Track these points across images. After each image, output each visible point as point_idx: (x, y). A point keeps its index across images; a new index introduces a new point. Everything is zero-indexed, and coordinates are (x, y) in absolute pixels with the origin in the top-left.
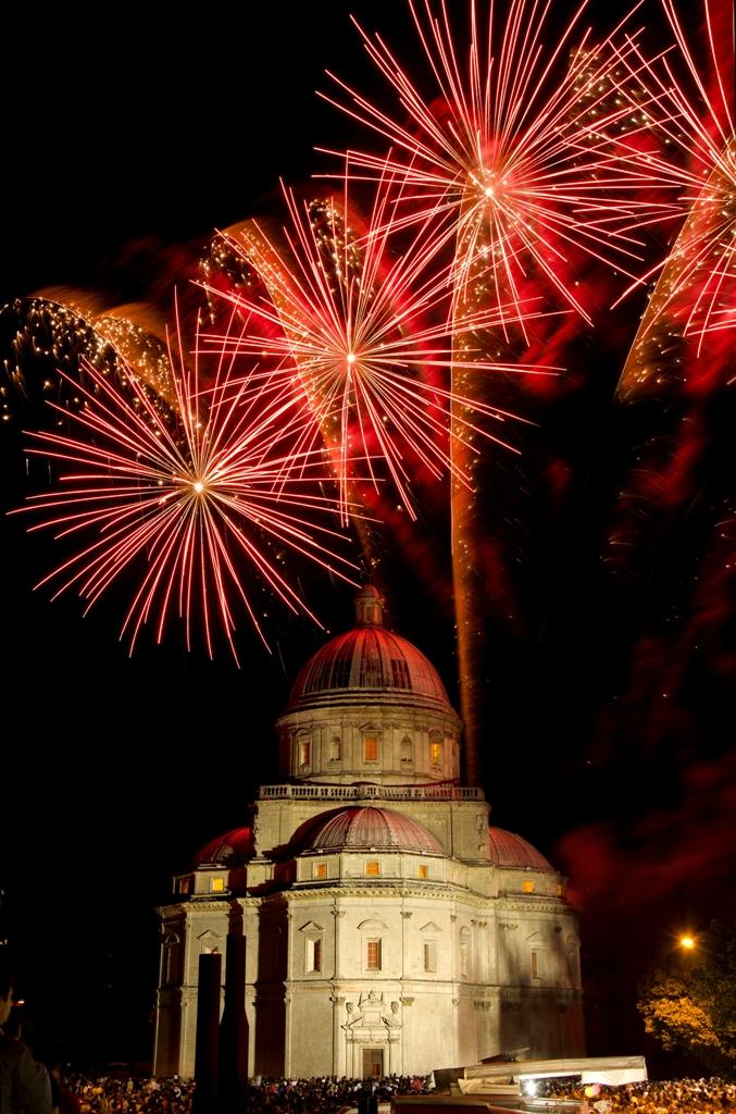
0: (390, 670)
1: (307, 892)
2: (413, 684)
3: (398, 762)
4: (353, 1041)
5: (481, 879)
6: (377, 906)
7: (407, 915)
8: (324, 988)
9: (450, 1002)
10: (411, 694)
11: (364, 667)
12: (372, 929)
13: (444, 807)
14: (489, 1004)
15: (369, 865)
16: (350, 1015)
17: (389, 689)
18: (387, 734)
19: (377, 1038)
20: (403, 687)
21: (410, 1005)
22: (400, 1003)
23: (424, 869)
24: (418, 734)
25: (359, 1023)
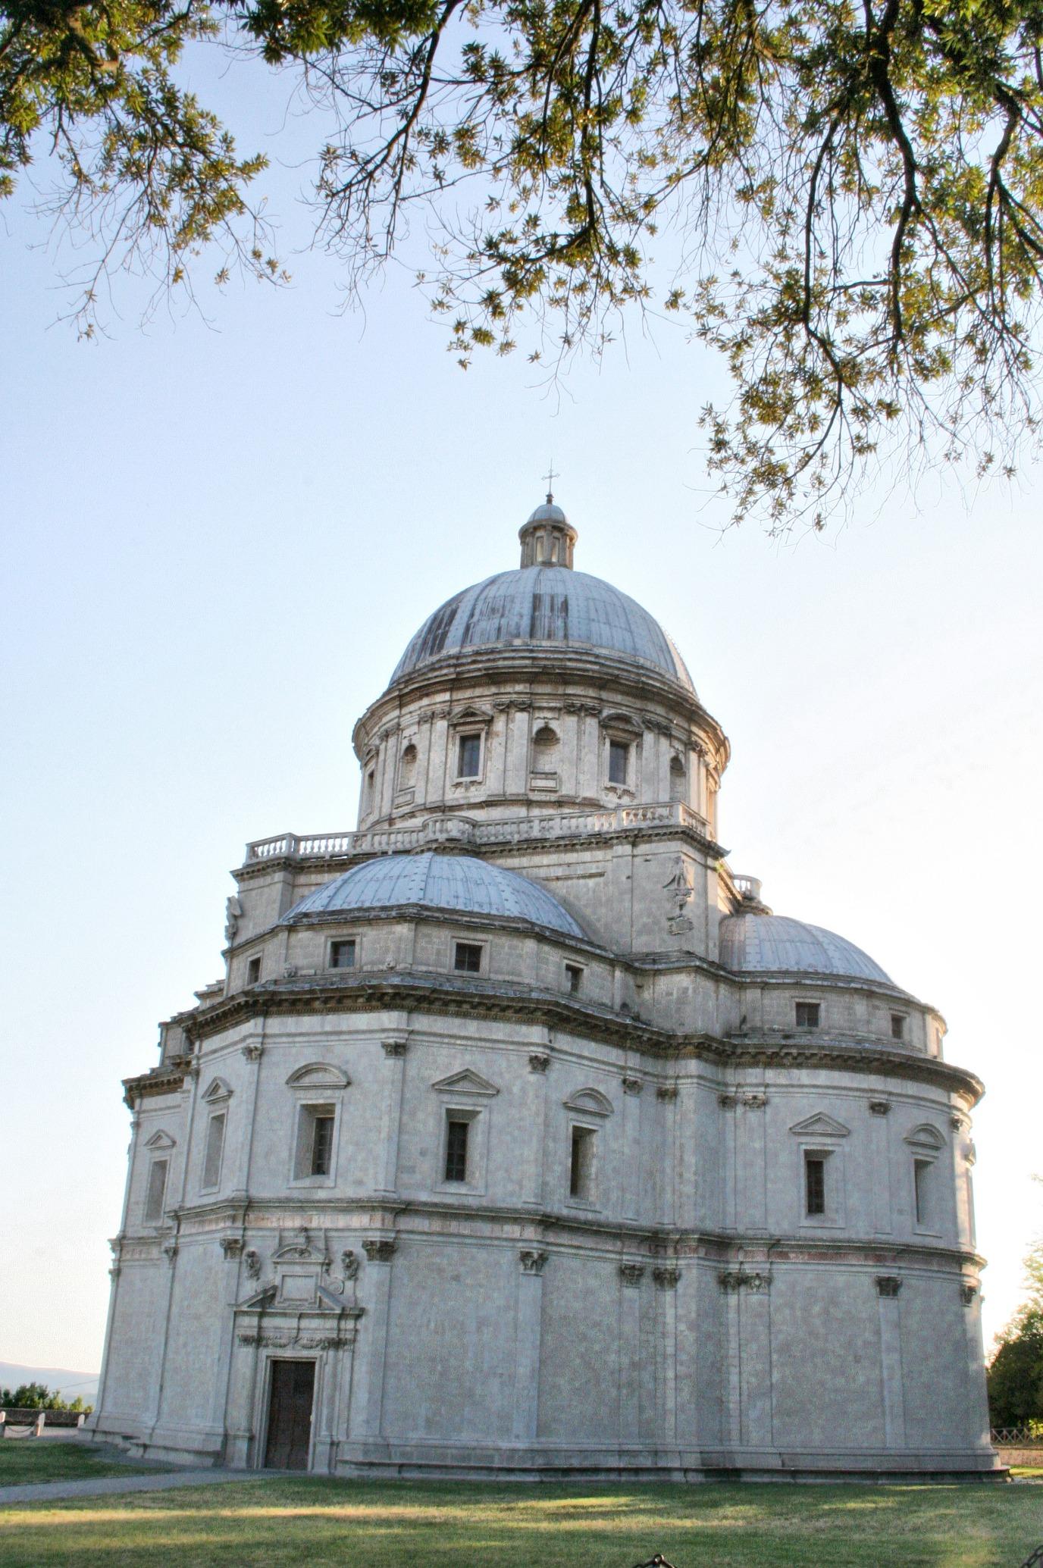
0: (526, 608)
2: (574, 631)
3: (523, 773)
4: (246, 1340)
5: (669, 994)
7: (397, 1050)
8: (217, 1221)
9: (508, 1258)
11: (477, 612)
12: (316, 1087)
15: (336, 947)
17: (517, 642)
18: (499, 725)
20: (549, 637)
21: (386, 1260)
22: (360, 1252)
23: (469, 957)
24: (571, 721)
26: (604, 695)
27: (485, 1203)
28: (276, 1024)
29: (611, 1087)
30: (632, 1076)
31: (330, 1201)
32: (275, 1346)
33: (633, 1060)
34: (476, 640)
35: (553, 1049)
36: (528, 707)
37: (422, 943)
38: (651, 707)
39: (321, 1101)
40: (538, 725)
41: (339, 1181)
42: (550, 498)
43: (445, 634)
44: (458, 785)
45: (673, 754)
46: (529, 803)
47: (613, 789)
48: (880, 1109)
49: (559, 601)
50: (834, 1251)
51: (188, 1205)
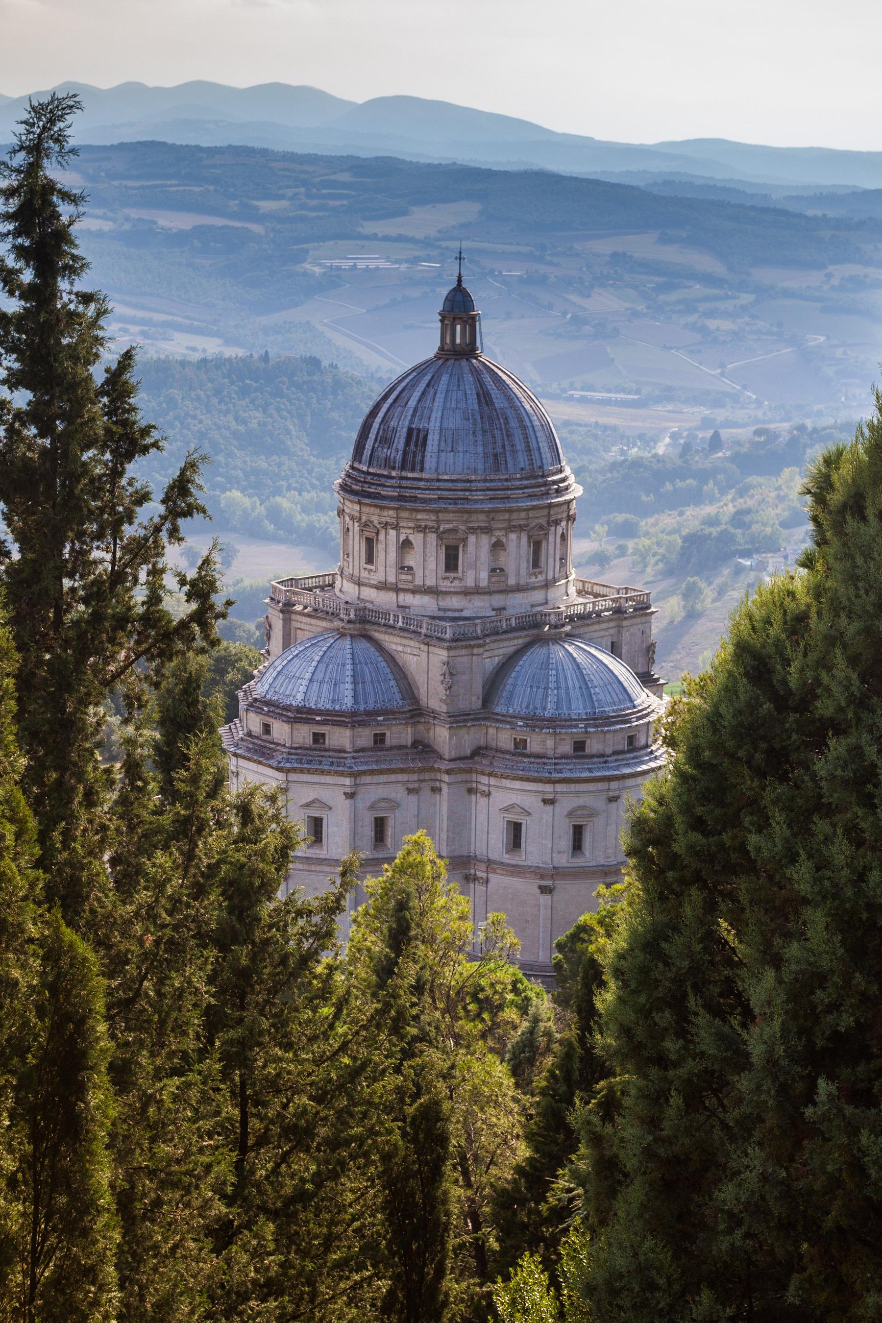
2: (427, 465)
10: (420, 480)
17: (394, 474)
18: (382, 537)
20: (413, 470)
23: (318, 738)
26: (440, 515)
27: (327, 857)
29: (398, 793)
30: (411, 786)
33: (415, 777)
36: (396, 527)
37: (295, 733)
38: (474, 517)
40: (402, 537)
42: (460, 280)
45: (494, 539)
46: (397, 590)
47: (446, 578)
49: (421, 437)
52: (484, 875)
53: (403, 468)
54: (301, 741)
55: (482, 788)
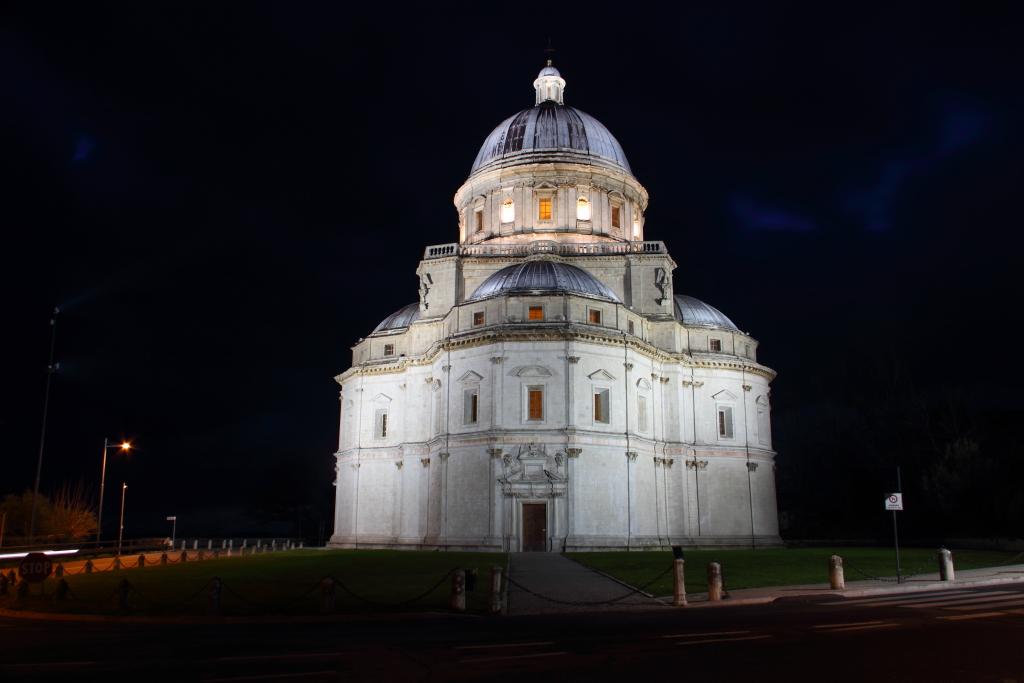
1: (461, 339)
4: (510, 495)
6: (537, 351)
8: (481, 440)
11: (538, 130)
13: (622, 262)
14: (671, 462)
15: (531, 309)
16: (508, 470)
17: (564, 149)
18: (561, 193)
19: (540, 492)
20: (580, 148)
22: (564, 454)
24: (595, 195)
25: (517, 477)
28: (507, 345)
31: (549, 430)
32: (524, 497)
34: (541, 143)
35: (633, 359)
39: (536, 384)
41: (550, 422)
43: (521, 142)
44: (541, 223)
48: (746, 388)
49: (580, 128)
50: (729, 452)
51: (451, 432)
52: (704, 459)
53: (571, 146)
54: (580, 316)
55: (696, 380)
